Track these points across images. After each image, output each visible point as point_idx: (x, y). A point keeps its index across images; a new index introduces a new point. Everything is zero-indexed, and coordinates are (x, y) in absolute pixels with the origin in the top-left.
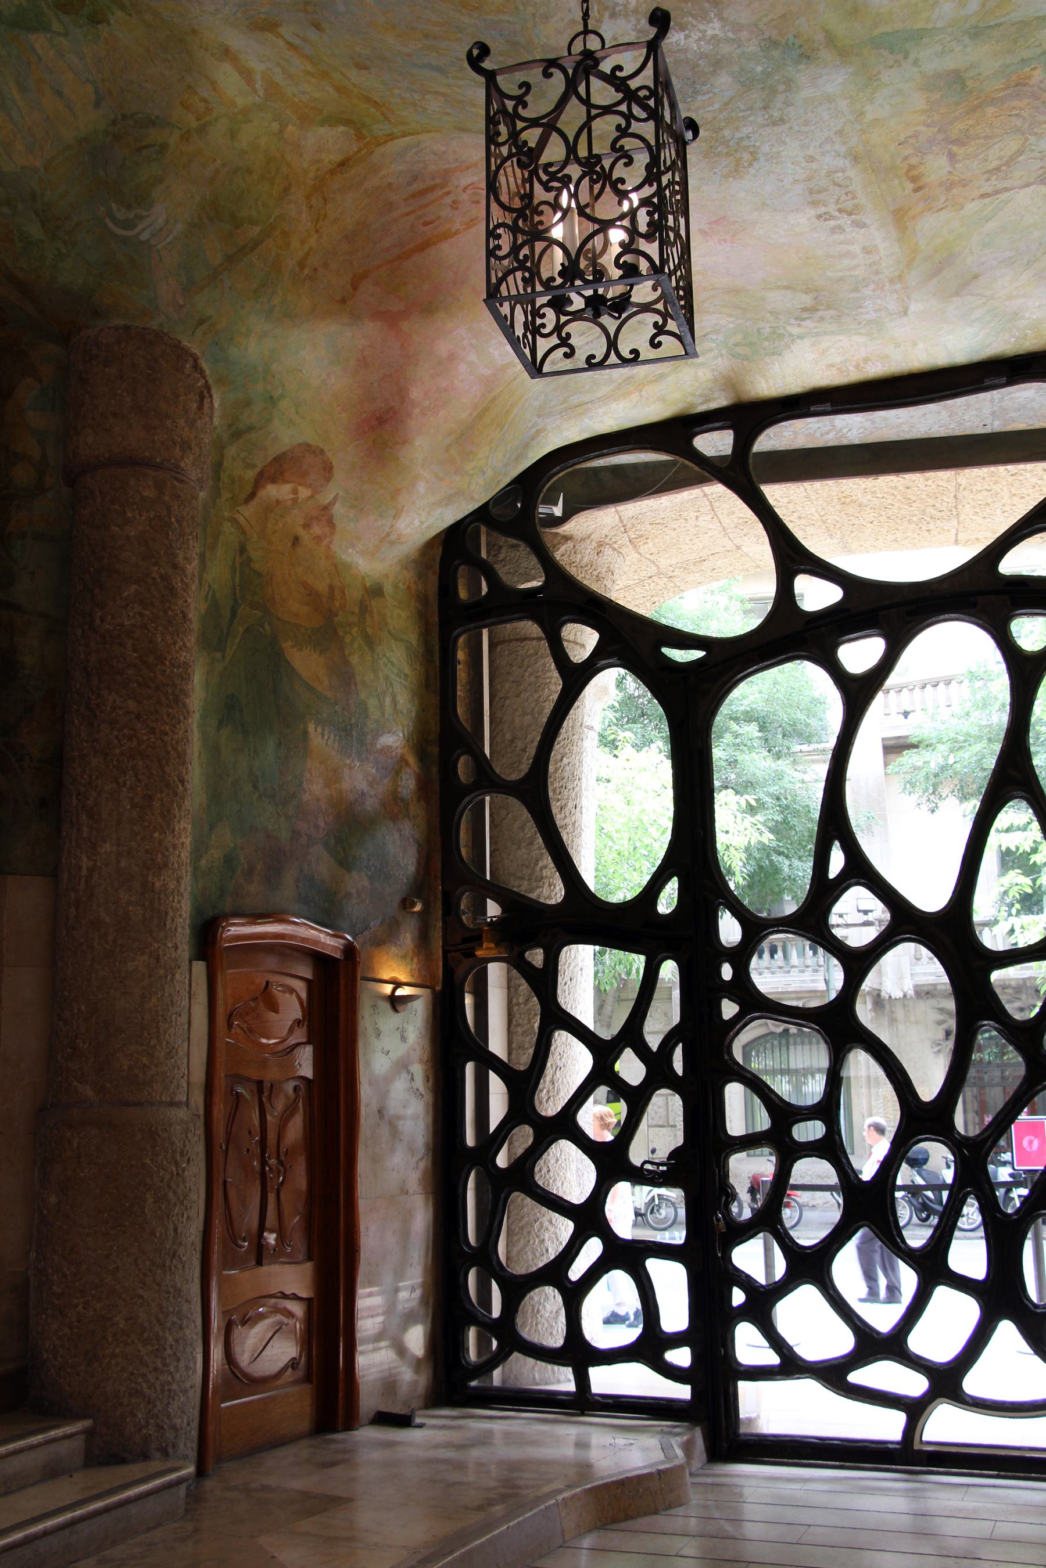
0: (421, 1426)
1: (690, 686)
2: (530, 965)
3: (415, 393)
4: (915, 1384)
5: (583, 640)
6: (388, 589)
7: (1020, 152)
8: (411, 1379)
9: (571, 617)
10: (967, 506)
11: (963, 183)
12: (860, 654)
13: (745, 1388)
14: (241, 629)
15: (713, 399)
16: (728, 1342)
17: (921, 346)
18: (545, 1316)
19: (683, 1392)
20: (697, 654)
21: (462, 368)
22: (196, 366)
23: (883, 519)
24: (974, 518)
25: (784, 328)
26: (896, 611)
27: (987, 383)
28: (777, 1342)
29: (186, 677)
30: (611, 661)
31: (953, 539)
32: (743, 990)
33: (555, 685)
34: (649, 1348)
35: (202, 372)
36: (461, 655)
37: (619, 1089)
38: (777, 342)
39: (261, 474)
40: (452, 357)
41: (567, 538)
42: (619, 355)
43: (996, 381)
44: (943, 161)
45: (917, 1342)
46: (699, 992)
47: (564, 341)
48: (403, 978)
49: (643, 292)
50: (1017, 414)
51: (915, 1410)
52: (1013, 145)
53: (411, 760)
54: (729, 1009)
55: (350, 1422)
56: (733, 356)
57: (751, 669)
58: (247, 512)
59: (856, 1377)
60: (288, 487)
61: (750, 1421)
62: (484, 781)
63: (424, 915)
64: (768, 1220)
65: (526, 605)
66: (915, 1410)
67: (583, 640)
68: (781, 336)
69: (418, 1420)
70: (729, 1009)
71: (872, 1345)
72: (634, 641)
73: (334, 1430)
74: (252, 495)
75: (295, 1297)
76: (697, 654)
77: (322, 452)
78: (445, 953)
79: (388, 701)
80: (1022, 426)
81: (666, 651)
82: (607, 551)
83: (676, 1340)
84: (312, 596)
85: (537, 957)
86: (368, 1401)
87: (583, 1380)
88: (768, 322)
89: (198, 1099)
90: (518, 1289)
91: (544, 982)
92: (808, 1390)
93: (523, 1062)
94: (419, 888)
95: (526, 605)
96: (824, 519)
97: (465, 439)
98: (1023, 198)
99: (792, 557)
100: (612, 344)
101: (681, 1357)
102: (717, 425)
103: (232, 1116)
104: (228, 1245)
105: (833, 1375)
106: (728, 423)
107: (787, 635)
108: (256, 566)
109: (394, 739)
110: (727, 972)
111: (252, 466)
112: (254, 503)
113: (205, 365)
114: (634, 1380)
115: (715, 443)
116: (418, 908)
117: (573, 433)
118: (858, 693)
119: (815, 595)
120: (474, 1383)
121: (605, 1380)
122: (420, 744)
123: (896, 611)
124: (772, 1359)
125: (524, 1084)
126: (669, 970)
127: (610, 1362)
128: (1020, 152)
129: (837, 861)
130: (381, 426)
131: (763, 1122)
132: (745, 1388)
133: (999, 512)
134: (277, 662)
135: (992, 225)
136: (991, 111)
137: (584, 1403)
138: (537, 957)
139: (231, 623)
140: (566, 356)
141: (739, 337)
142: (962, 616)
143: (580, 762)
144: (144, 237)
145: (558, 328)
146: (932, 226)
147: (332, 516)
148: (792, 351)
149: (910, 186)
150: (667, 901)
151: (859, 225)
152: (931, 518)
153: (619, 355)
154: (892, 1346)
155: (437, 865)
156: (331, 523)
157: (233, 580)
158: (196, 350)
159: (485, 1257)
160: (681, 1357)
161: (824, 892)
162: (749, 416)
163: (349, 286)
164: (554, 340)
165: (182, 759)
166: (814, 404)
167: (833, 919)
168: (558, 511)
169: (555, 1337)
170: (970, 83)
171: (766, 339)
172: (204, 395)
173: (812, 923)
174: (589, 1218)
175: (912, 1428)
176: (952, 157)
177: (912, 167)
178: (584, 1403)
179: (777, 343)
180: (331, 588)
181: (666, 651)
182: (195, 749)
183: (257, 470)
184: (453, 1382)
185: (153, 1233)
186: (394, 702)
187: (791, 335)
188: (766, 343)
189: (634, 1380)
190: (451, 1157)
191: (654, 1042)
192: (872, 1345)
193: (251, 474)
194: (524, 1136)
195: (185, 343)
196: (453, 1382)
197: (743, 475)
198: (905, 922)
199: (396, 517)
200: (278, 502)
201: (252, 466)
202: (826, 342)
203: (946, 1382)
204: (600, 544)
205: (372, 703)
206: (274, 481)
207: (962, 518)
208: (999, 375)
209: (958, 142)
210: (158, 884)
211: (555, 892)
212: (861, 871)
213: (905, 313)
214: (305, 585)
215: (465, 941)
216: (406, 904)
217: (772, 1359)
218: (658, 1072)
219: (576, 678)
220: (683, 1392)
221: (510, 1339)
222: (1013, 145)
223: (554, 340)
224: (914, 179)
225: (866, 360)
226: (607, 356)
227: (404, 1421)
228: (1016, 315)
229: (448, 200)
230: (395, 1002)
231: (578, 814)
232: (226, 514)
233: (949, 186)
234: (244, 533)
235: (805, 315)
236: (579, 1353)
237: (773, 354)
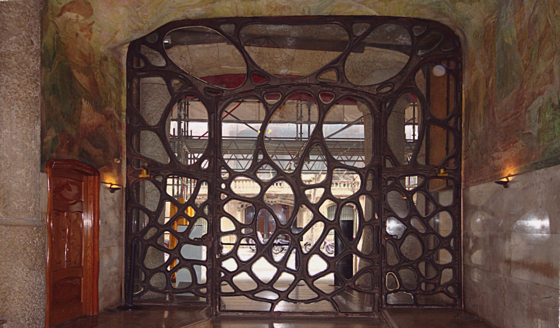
4: (273, 296)
14: (57, 62)
39: (64, 7)
51: (274, 303)
54: (224, 196)
58: (58, 20)
59: (256, 295)
60: (75, 14)
64: (233, 254)
66: (274, 303)
71: (262, 286)
74: (60, 15)
84: (82, 55)
105: (251, 294)
108: (62, 40)
110: (223, 186)
111: (61, 4)
112: (61, 17)
129: (261, 157)
131: (233, 228)
134: (71, 76)
139: (53, 59)
147: (91, 29)
150: (205, 164)
157: (54, 43)
180: (90, 54)
183: (62, 5)
200: (70, 19)
201: (61, 4)
206: (69, 11)
214: (80, 51)
232: (50, 19)
234: (57, 27)
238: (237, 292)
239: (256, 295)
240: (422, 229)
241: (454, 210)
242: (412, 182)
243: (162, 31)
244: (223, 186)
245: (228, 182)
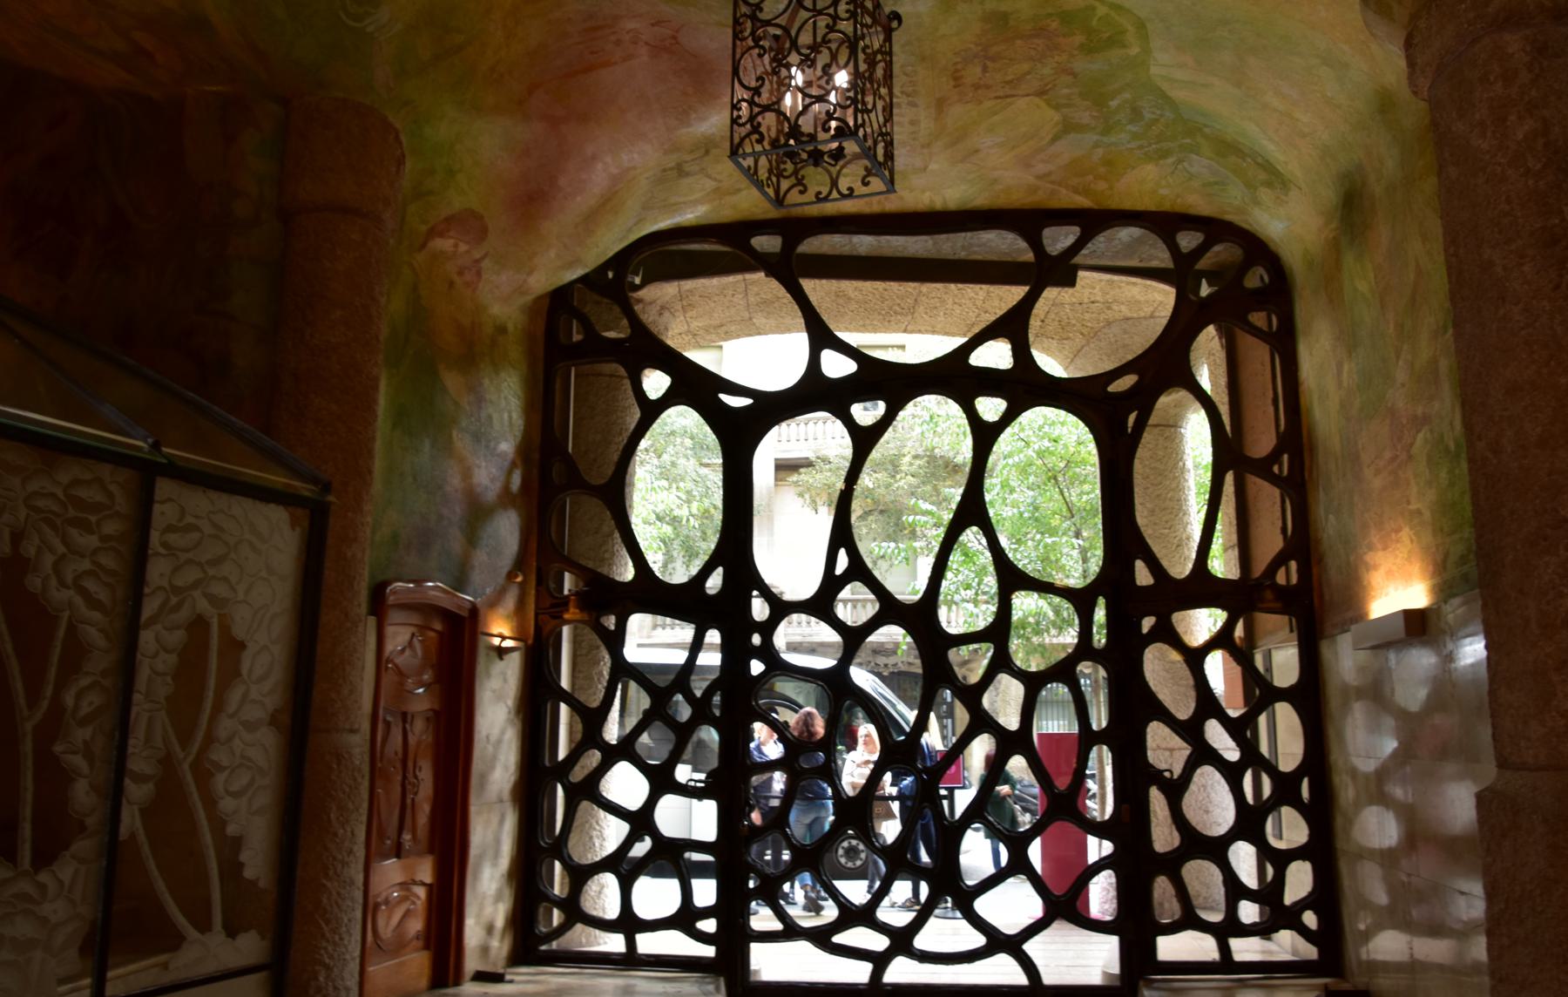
0: (511, 982)
1: (740, 426)
2: (606, 629)
3: (562, 181)
4: (879, 943)
5: (656, 383)
6: (510, 327)
7: (1029, 73)
8: (500, 947)
11: (988, 87)
12: (866, 413)
13: (755, 948)
16: (746, 914)
17: (928, 194)
18: (605, 895)
19: (709, 951)
20: (749, 401)
21: (600, 166)
22: (397, 138)
26: (895, 384)
28: (781, 915)
29: (376, 388)
32: (768, 653)
33: (636, 414)
34: (685, 919)
35: (401, 143)
36: (558, 386)
37: (671, 723)
40: (594, 158)
41: (640, 301)
42: (839, 192)
44: (978, 70)
45: (884, 914)
46: (735, 652)
47: (800, 182)
48: (507, 633)
49: (851, 147)
51: (881, 961)
52: (1026, 67)
53: (519, 462)
54: (757, 667)
55: (458, 981)
59: (838, 939)
61: (757, 972)
62: (574, 484)
63: (522, 585)
65: (614, 350)
67: (656, 383)
69: (508, 977)
70: (757, 667)
71: (852, 916)
72: (697, 387)
73: (445, 985)
75: (423, 884)
76: (749, 401)
77: (482, 217)
78: (537, 615)
79: (506, 416)
80: (979, 257)
81: (722, 396)
82: (667, 314)
83: (706, 913)
85: (610, 622)
86: (471, 964)
87: (631, 943)
89: (366, 726)
90: (580, 875)
91: (615, 641)
92: (804, 947)
93: (595, 702)
94: (520, 564)
95: (614, 350)
97: (591, 220)
98: (1022, 103)
99: (821, 337)
100: (834, 184)
101: (709, 925)
103: (385, 740)
104: (384, 845)
105: (822, 938)
107: (814, 394)
109: (507, 447)
113: (404, 139)
114: (674, 943)
115: (767, 243)
116: (519, 579)
117: (664, 224)
118: (864, 440)
119: (836, 366)
120: (543, 948)
121: (648, 944)
122: (524, 451)
123: (895, 384)
124: (777, 926)
125: (592, 720)
126: (713, 636)
127: (653, 930)
128: (1029, 73)
130: (532, 200)
132: (755, 948)
135: (996, 118)
136: (1019, 42)
137: (631, 960)
138: (610, 622)
140: (801, 192)
144: (370, 29)
145: (796, 172)
146: (957, 113)
149: (952, 83)
150: (714, 583)
151: (913, 105)
153: (839, 192)
154: (863, 916)
155: (533, 546)
156: (479, 274)
158: (398, 126)
159: (559, 848)
160: (709, 925)
161: (832, 584)
162: (795, 228)
164: (793, 180)
165: (370, 454)
167: (877, 606)
168: (637, 280)
169: (612, 910)
170: (1012, 23)
172: (400, 161)
173: (821, 606)
174: (641, 821)
175: (877, 973)
176: (985, 69)
177: (957, 71)
178: (631, 960)
181: (722, 396)
182: (379, 446)
184: (529, 944)
185: (336, 834)
186: (510, 417)
189: (674, 943)
190: (536, 774)
191: (698, 693)
192: (852, 916)
193: (423, 228)
194: (594, 757)
195: (391, 119)
196: (529, 944)
197: (789, 271)
198: (890, 609)
199: (530, 273)
203: (902, 941)
204: (663, 308)
205: (495, 416)
209: (993, 59)
210: (349, 554)
211: (628, 573)
212: (859, 571)
215: (553, 606)
216: (510, 576)
217: (777, 926)
218: (702, 713)
219: (652, 410)
220: (709, 951)
221: (575, 913)
222: (1026, 67)
223: (793, 180)
224: (956, 79)
226: (830, 193)
227: (497, 978)
228: (995, 181)
229: (613, 38)
230: (501, 652)
233: (977, 87)
236: (629, 923)
238: (791, 932)
239: (838, 939)
240: (1232, 754)
241: (1310, 696)
242: (1202, 623)
243: (623, 260)
244: (756, 639)
245: (768, 628)
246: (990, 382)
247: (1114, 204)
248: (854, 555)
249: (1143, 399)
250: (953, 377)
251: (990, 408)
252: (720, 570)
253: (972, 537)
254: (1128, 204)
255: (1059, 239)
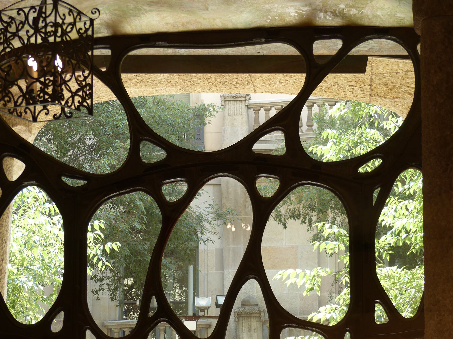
9: (9, 153)
10: (258, 79)
15: (100, 33)
23: (206, 83)
24: (263, 85)
25: (142, 7)
27: (255, 41)
30: (32, 182)
31: (253, 91)
38: (138, 12)
43: (259, 40)
50: (277, 49)
56: (112, 14)
57: (112, 195)
68: (139, 10)
88: (132, 3)
96: (169, 81)
102: (101, 46)
106: (108, 46)
133: (278, 83)
141: (116, 7)
142: (230, 175)
143: (7, 231)
148: (146, 16)
150: (57, 325)
152: (236, 83)
163: (13, 267)
166: (158, 41)
171: (131, 10)
179: (137, 12)
187: (145, 9)
188: (132, 11)
202: (164, 14)
207: (256, 84)
208: (261, 37)
213: (207, 9)
225: (188, 23)
231: (4, 264)
235: (152, 4)
237: (135, 16)
246: (268, 164)
247: (366, 22)
248: (162, 300)
249: (384, 181)
250: (240, 161)
251: (267, 186)
252: (62, 314)
253: (251, 288)
254: (377, 23)
255: (325, 48)
